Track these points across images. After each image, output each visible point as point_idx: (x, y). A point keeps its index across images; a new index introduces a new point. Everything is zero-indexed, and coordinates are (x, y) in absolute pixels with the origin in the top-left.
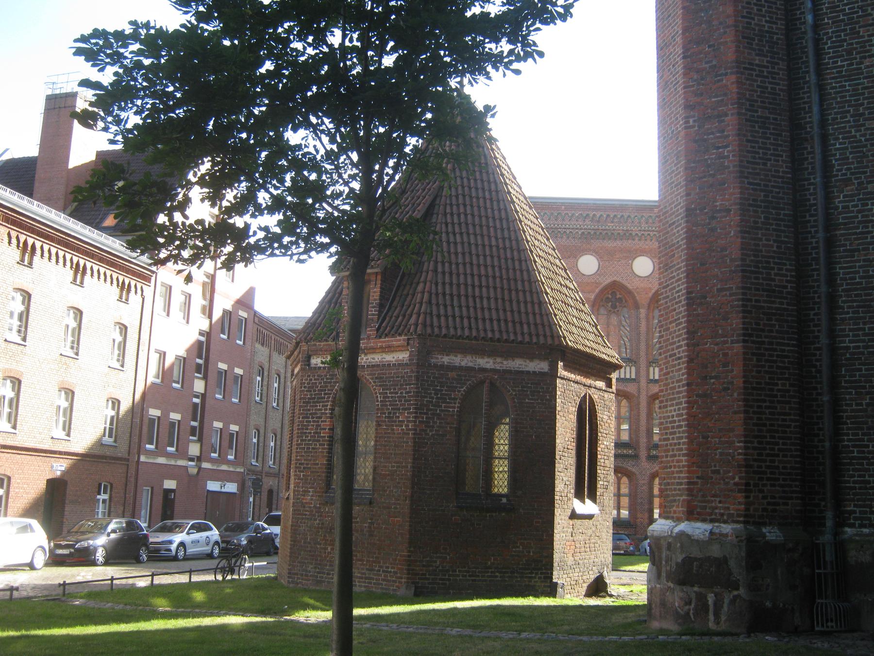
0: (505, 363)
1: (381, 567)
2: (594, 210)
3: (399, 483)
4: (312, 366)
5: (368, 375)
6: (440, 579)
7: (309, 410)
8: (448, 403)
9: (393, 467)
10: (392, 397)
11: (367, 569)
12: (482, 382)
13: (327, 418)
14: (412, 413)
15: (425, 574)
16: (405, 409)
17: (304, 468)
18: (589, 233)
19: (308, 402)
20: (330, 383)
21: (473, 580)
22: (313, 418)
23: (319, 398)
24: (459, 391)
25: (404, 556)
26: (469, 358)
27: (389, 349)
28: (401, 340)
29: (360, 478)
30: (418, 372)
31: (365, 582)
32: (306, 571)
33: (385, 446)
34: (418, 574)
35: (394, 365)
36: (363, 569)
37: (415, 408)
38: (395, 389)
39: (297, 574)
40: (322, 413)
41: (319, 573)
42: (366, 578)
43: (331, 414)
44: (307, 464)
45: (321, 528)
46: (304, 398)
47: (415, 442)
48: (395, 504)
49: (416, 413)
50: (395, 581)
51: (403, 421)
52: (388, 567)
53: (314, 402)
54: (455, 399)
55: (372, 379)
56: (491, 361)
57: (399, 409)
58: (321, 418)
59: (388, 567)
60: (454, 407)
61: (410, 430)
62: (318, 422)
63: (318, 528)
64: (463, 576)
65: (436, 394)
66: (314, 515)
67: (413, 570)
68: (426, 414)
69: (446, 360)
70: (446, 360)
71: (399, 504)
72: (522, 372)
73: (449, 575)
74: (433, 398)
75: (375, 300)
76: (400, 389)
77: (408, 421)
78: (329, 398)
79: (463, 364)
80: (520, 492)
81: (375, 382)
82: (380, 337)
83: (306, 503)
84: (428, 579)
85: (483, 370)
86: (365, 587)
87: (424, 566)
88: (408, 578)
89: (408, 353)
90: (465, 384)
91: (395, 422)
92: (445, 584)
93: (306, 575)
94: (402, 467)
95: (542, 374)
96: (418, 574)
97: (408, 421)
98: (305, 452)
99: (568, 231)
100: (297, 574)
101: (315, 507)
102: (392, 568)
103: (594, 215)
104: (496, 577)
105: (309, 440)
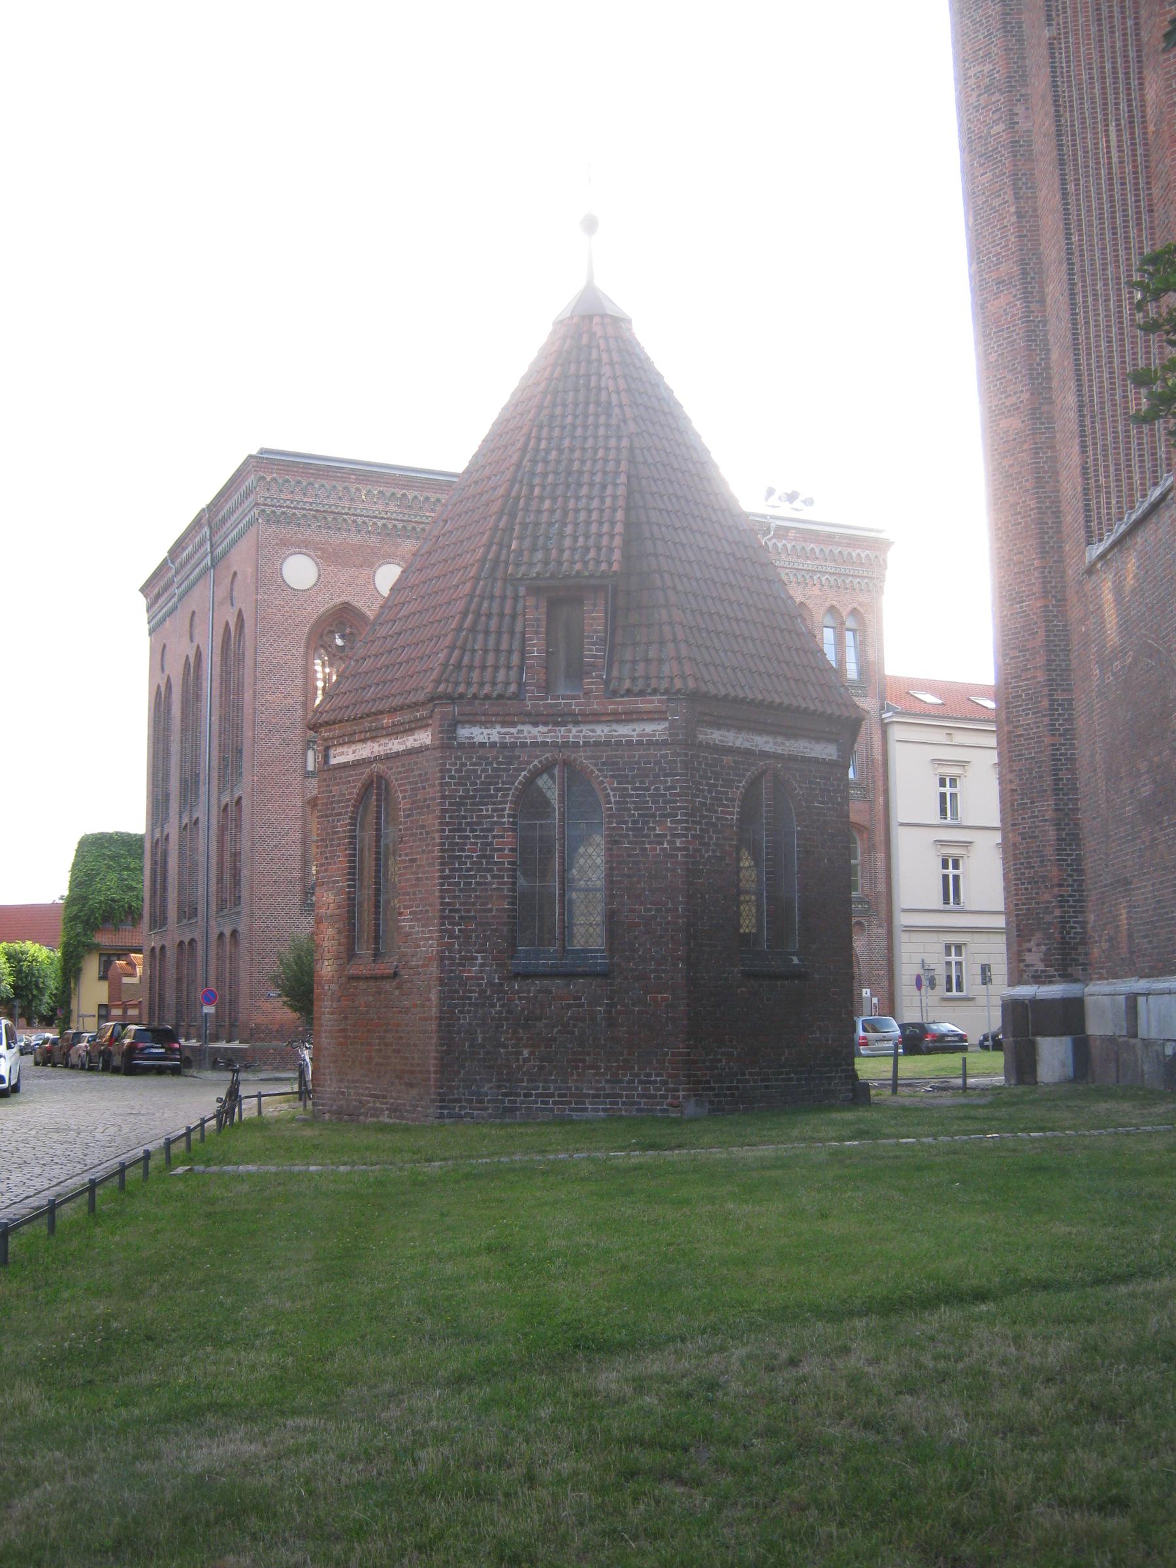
0: (787, 743)
1: (638, 1075)
2: (404, 487)
3: (661, 937)
6: (728, 1088)
7: (464, 817)
8: (727, 806)
9: (647, 910)
10: (638, 796)
11: (607, 1081)
12: (763, 773)
13: (507, 830)
14: (680, 822)
15: (708, 1082)
17: (461, 918)
18: (395, 526)
21: (767, 1087)
22: (473, 830)
23: (482, 797)
24: (737, 788)
25: (680, 1054)
26: (744, 735)
27: (630, 717)
28: (654, 703)
29: (579, 931)
30: (686, 755)
31: (605, 1103)
33: (629, 876)
34: (700, 1082)
35: (640, 743)
36: (598, 1081)
37: (686, 815)
38: (642, 782)
39: (459, 1101)
42: (607, 1096)
43: (514, 823)
44: (468, 911)
45: (507, 1019)
46: (450, 797)
47: (688, 869)
49: (686, 821)
50: (665, 1097)
53: (472, 804)
54: (733, 800)
55: (596, 765)
56: (770, 739)
57: (654, 816)
58: (491, 830)
59: (649, 1075)
60: (732, 813)
61: (680, 849)
62: (487, 837)
63: (500, 1019)
64: (755, 1081)
65: (710, 792)
66: (490, 998)
67: (694, 1075)
68: (699, 823)
69: (716, 736)
70: (716, 736)
71: (664, 971)
72: (810, 760)
73: (739, 1081)
74: (705, 797)
75: (596, 631)
76: (652, 783)
77: (673, 836)
78: (507, 795)
79: (738, 744)
80: (814, 947)
82: (615, 693)
83: (468, 978)
84: (713, 1089)
85: (765, 755)
86: (605, 1110)
87: (707, 1068)
88: (689, 1090)
89: (667, 724)
90: (744, 776)
91: (648, 836)
92: (733, 1095)
93: (482, 1102)
95: (832, 764)
96: (700, 1082)
97: (673, 836)
98: (460, 891)
99: (359, 520)
100: (459, 1101)
101: (490, 983)
103: (404, 495)
104: (791, 1079)
105: (468, 870)
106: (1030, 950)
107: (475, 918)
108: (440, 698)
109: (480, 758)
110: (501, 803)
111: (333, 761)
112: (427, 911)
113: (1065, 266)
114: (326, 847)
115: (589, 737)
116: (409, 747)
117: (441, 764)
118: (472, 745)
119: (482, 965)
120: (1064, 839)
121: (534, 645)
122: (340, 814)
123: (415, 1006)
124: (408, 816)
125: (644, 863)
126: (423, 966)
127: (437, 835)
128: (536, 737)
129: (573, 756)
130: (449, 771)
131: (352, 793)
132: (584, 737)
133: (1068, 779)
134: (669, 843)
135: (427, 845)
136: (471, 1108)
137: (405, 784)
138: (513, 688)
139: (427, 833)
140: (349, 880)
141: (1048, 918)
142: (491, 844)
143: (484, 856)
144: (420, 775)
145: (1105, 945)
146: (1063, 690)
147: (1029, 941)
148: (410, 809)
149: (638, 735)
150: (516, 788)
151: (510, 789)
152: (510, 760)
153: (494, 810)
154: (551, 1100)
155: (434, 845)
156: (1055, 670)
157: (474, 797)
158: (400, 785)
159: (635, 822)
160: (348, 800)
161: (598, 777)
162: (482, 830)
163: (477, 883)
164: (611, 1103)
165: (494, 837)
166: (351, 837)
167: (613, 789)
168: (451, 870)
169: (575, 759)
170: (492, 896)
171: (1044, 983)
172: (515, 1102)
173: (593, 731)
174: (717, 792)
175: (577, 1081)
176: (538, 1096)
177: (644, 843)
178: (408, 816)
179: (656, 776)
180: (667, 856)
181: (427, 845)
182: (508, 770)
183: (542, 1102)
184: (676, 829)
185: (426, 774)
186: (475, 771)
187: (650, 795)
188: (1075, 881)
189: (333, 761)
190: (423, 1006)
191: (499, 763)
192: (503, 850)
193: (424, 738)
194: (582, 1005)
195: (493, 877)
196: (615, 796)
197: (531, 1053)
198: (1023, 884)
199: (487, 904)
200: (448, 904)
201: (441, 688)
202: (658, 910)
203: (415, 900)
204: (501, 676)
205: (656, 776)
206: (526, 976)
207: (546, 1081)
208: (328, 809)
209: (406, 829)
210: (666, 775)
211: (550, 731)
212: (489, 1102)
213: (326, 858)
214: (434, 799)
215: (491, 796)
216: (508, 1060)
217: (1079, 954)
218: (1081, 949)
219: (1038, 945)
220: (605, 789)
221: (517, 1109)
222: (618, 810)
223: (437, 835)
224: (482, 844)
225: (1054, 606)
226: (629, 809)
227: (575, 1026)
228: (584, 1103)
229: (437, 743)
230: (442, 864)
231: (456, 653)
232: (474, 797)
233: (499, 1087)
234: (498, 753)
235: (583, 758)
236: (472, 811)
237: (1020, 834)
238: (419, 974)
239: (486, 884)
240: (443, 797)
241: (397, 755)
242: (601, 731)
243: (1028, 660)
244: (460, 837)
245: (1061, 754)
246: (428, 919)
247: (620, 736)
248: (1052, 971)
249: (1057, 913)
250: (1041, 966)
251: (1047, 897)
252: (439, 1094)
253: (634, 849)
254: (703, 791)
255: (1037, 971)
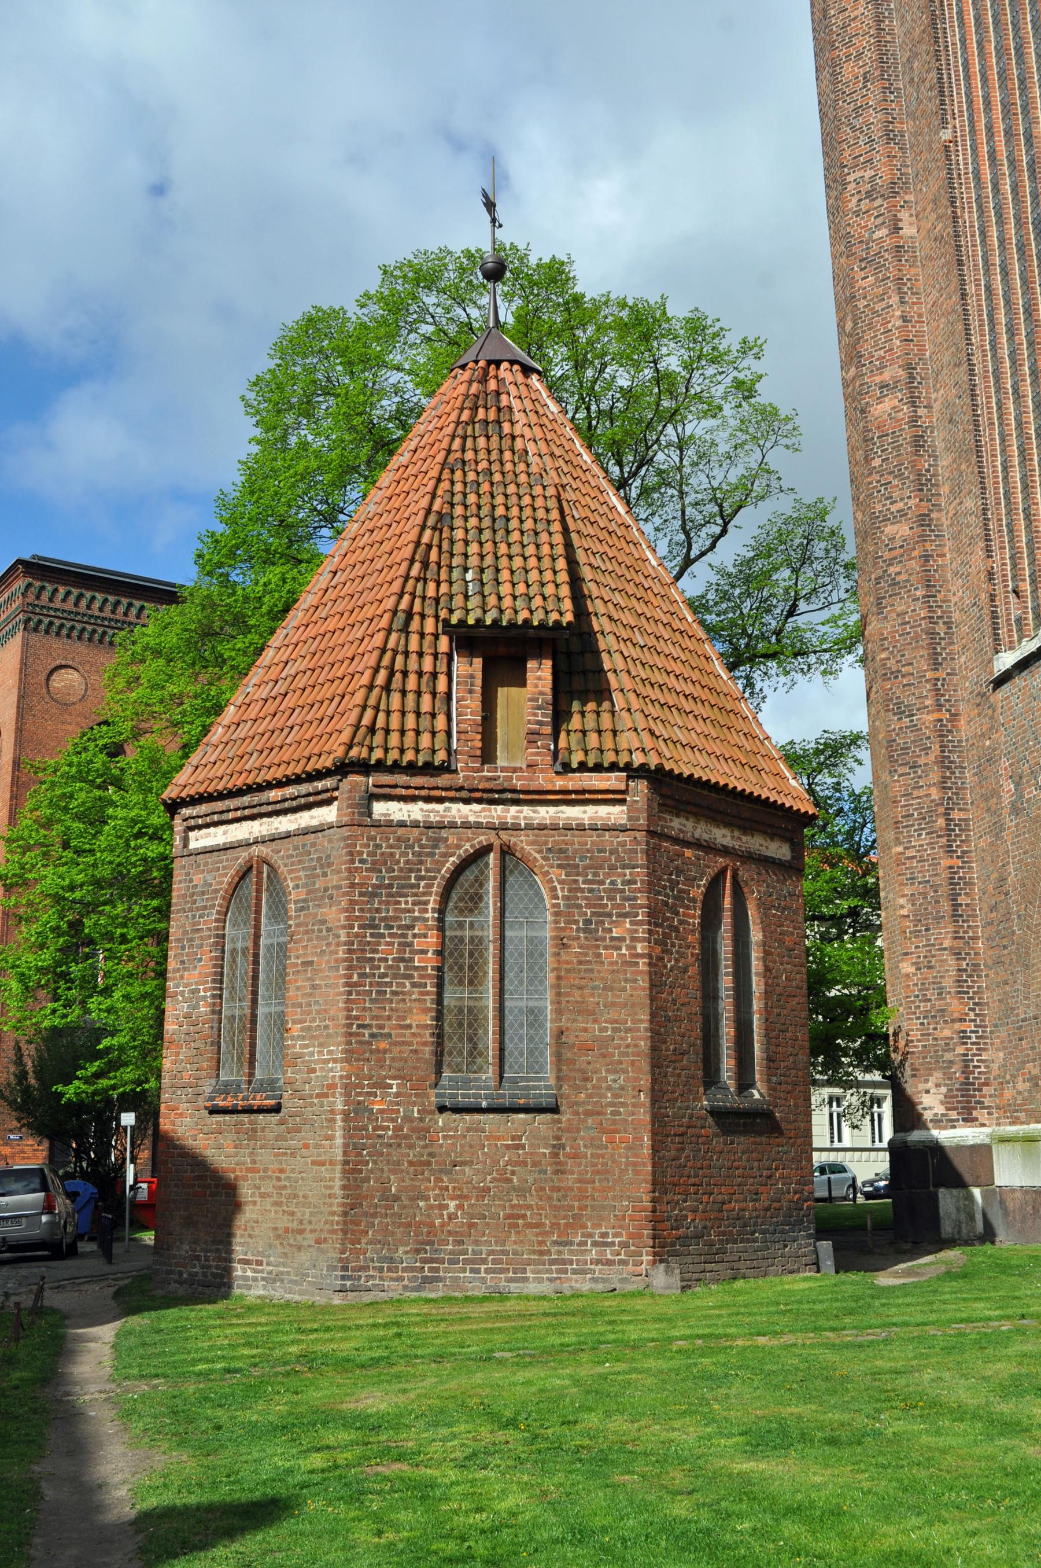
0: (744, 838)
1: (590, 1235)
3: (620, 1062)
4: (375, 816)
5: (532, 843)
7: (378, 911)
9: (606, 1029)
10: (591, 891)
16: (626, 915)
19: (373, 895)
20: (432, 855)
24: (699, 886)
26: (702, 826)
28: (613, 781)
31: (550, 1271)
32: (391, 1260)
36: (540, 1243)
38: (595, 874)
39: (366, 1268)
40: (416, 919)
41: (424, 1261)
42: (553, 1262)
44: (381, 1027)
46: (361, 885)
48: (612, 1104)
51: (623, 939)
52: (605, 1235)
55: (540, 852)
56: (725, 831)
57: (610, 915)
58: (412, 927)
59: (605, 1235)
61: (641, 956)
62: (405, 936)
75: (542, 693)
76: (608, 875)
78: (431, 886)
81: (545, 859)
82: (567, 768)
86: (550, 1280)
91: (604, 939)
94: (628, 1030)
97: (634, 939)
98: (372, 1001)
102: (615, 1235)
105: (385, 975)
106: (927, 1092)
107: (390, 1035)
108: (352, 764)
109: (399, 839)
110: (424, 894)
111: (193, 845)
112: (326, 1027)
113: (965, 367)
114: (183, 948)
115: (531, 818)
116: (303, 825)
117: (348, 846)
118: (389, 824)
119: (397, 1095)
120: (965, 970)
121: (467, 707)
122: (205, 908)
123: (306, 1146)
124: (302, 909)
125: (599, 971)
126: (318, 1096)
127: (342, 932)
128: (467, 816)
129: (513, 840)
130: (361, 853)
131: (221, 883)
132: (525, 818)
133: (967, 905)
134: (628, 948)
135: (329, 945)
136: (381, 1279)
137: (298, 871)
138: (441, 756)
139: (329, 930)
140: (214, 989)
141: (948, 1056)
142: (411, 944)
143: (403, 960)
144: (319, 859)
145: (1022, 1086)
146: (960, 810)
147: (927, 1081)
148: (305, 901)
149: (590, 818)
150: (443, 877)
151: (435, 878)
152: (436, 842)
153: (414, 904)
154: (483, 1267)
155: (338, 944)
156: (950, 788)
157: (391, 886)
158: (290, 872)
159: (587, 922)
160: (216, 891)
161: (542, 866)
162: (399, 927)
163: (395, 993)
164: (558, 1271)
165: (415, 936)
166: (217, 936)
167: (560, 882)
168: (360, 975)
169: (515, 844)
170: (410, 1009)
171: (945, 1128)
172: (437, 1270)
173: (534, 812)
174: (680, 891)
175: (515, 1243)
176: (466, 1262)
177: (598, 947)
178: (302, 909)
179: (613, 868)
180: (625, 963)
181: (329, 945)
182: (432, 855)
183: (472, 1271)
184: (636, 931)
185: (328, 856)
186: (392, 855)
187: (605, 890)
188: (976, 1015)
189: (193, 845)
190: (317, 1146)
191: (421, 846)
192: (426, 952)
193: (328, 814)
194: (523, 1147)
195: (414, 985)
196: (562, 889)
197: (459, 1207)
198: (918, 1018)
199: (404, 1018)
200: (357, 1018)
201: (354, 752)
202: (614, 1030)
203: (309, 1013)
204: (425, 740)
205: (613, 868)
206: (457, 1110)
207: (476, 1243)
208: (186, 902)
209: (298, 925)
210: (624, 867)
211: (483, 810)
212: (404, 1270)
213: (183, 962)
214: (339, 887)
215: (412, 886)
216: (429, 1216)
217: (984, 1096)
218: (985, 1089)
219: (938, 1086)
220: (551, 881)
221: (439, 1279)
222: (568, 906)
223: (342, 932)
224: (399, 944)
225: (948, 720)
226: (579, 906)
227: (513, 1173)
228: (524, 1271)
229: (345, 819)
230: (349, 968)
231: (369, 713)
232: (391, 886)
233: (418, 1251)
234: (421, 834)
235: (523, 843)
236: (388, 903)
237: (913, 964)
238: (312, 1105)
239: (403, 993)
240: (352, 885)
241: (288, 836)
242: (545, 814)
243: (920, 777)
244: (372, 935)
245: (960, 878)
246: (328, 1036)
247: (568, 818)
248: (953, 1115)
249: (960, 1050)
250: (940, 1110)
251: (947, 1033)
252: (341, 1260)
253: (586, 955)
254: (664, 887)
255: (936, 1115)
